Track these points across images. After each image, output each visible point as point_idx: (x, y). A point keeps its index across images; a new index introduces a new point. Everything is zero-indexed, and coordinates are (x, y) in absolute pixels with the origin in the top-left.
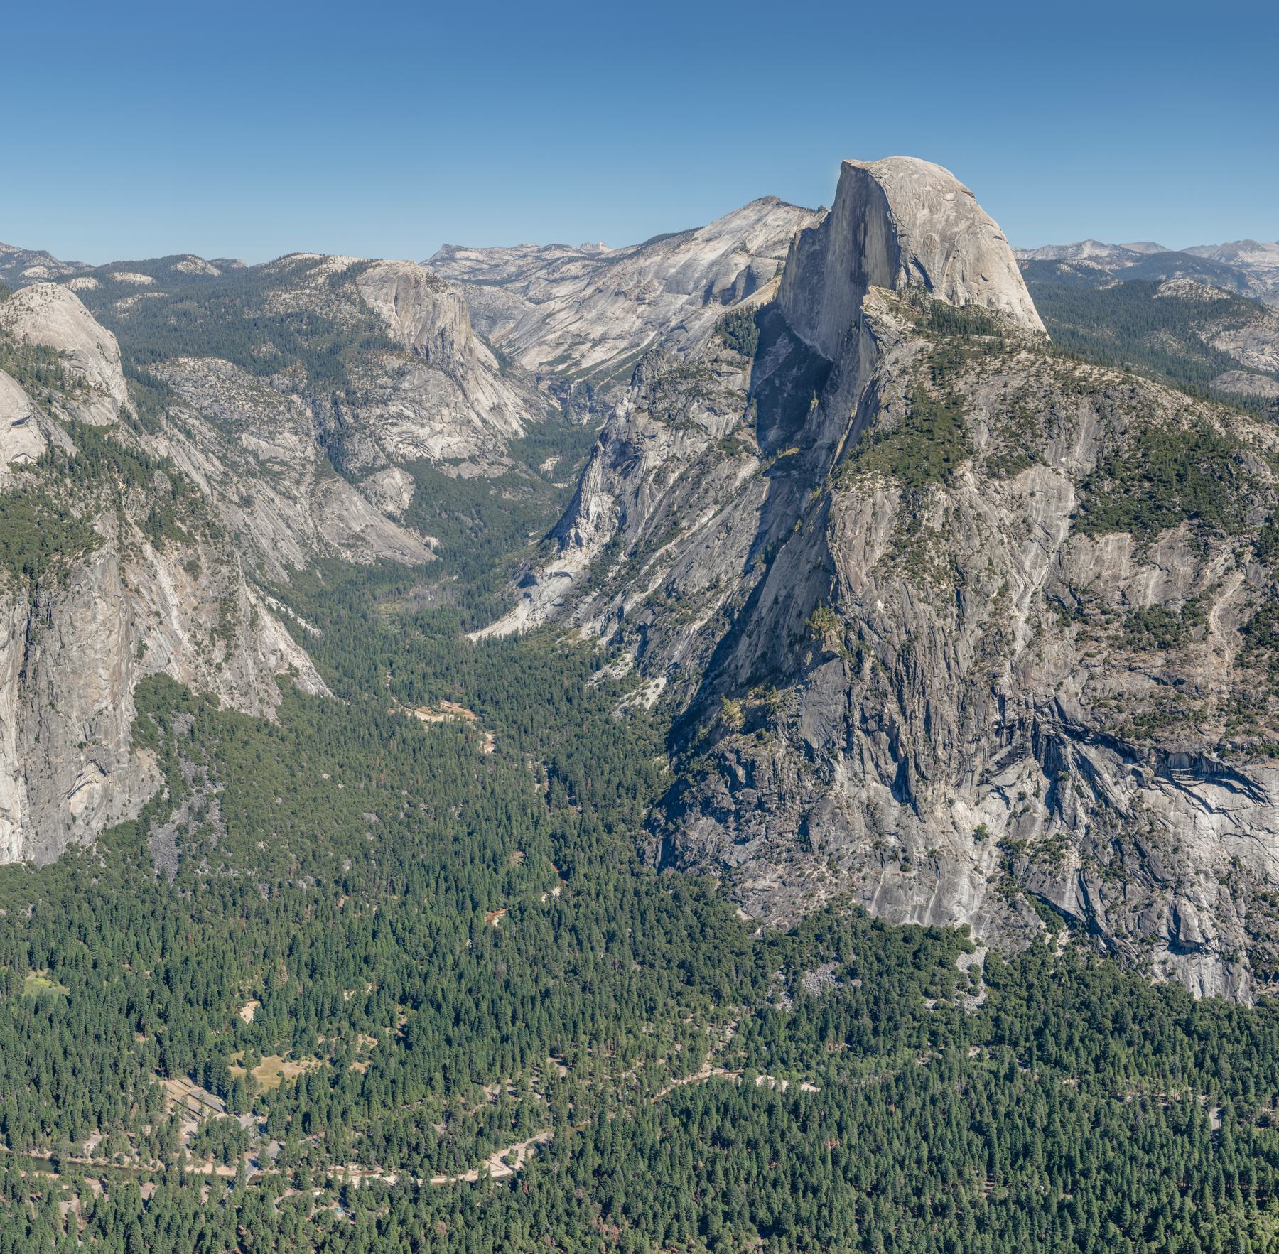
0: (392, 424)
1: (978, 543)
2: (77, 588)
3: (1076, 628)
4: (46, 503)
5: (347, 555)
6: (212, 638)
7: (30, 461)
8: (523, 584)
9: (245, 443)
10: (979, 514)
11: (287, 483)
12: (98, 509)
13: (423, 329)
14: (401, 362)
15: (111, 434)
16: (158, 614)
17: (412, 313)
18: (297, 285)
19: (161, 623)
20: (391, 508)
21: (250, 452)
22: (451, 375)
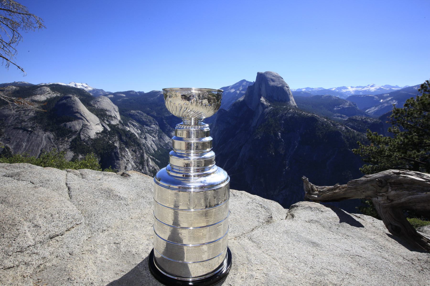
4: (104, 140)
7: (100, 132)
11: (153, 134)
12: (115, 141)
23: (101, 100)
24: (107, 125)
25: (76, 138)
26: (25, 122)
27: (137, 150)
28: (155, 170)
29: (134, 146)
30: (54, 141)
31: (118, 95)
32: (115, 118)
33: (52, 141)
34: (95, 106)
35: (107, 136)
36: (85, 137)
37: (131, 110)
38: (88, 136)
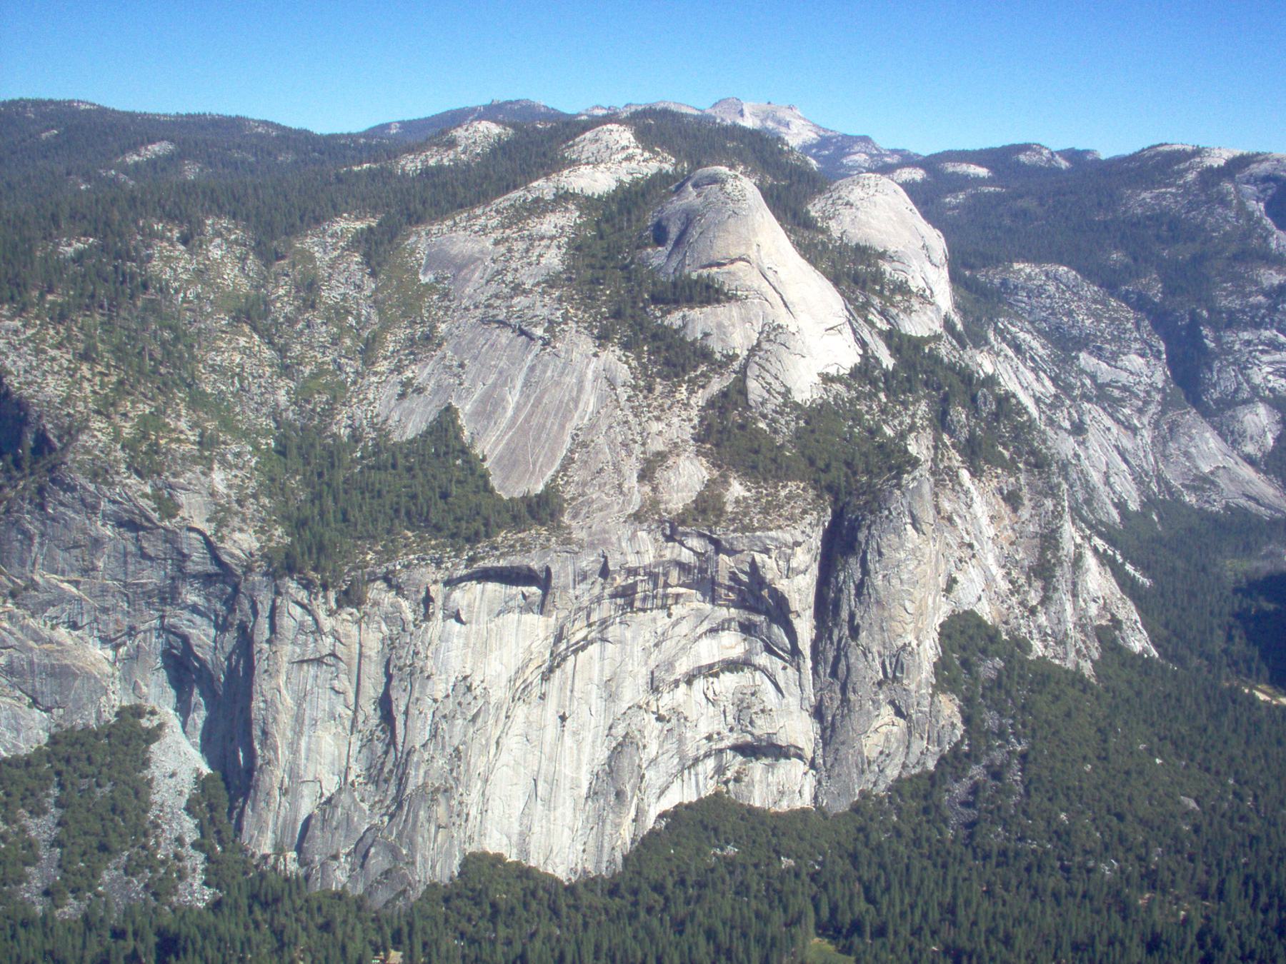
0: (1262, 352)
4: (857, 418)
5: (1190, 499)
6: (1028, 578)
7: (842, 372)
11: (1127, 411)
12: (912, 428)
15: (933, 345)
18: (1159, 182)
19: (974, 556)
20: (1250, 448)
21: (1085, 372)
23: (862, 195)
24: (881, 333)
25: (724, 394)
26: (524, 291)
28: (1116, 623)
29: (1010, 467)
30: (629, 399)
31: (950, 168)
32: (926, 298)
33: (623, 393)
34: (828, 227)
35: (876, 395)
36: (768, 391)
37: (1011, 262)
38: (783, 390)
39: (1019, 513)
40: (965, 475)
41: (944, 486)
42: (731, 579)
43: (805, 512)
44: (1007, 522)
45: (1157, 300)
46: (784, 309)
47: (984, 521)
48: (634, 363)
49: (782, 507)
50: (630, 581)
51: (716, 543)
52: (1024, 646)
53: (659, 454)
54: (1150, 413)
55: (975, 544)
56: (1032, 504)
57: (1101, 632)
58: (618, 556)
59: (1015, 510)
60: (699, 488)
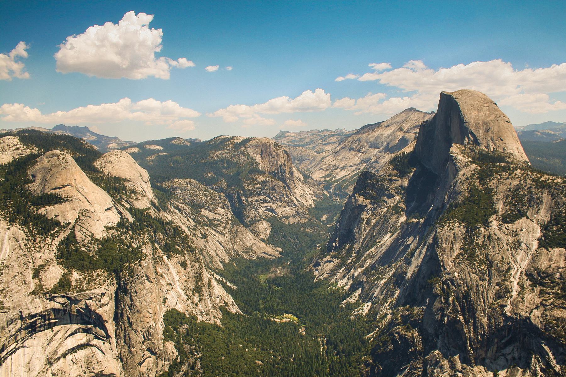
0: (262, 203)
1: (498, 250)
2: (137, 276)
3: (538, 289)
4: (122, 242)
5: (245, 256)
6: (193, 293)
7: (114, 225)
8: (314, 266)
9: (203, 213)
10: (498, 238)
12: (143, 243)
13: (272, 165)
14: (264, 178)
16: (171, 284)
17: (268, 158)
19: (172, 288)
20: (262, 236)
21: (205, 216)
22: (285, 183)
23: (115, 158)
24: (127, 209)
27: (188, 262)
28: (226, 304)
29: (182, 253)
30: (25, 245)
31: (148, 147)
32: (143, 194)
35: (128, 232)
36: (85, 236)
38: (91, 234)
39: (187, 270)
40: (165, 258)
41: (158, 263)
42: (77, 312)
43: (105, 281)
44: (183, 273)
45: (225, 189)
46: (88, 203)
47: (174, 274)
48: (26, 230)
49: (96, 280)
50: (33, 320)
51: (69, 298)
52: (195, 318)
53: (41, 265)
54: (228, 228)
55: (172, 283)
56: (191, 265)
57: (221, 308)
58: (27, 311)
59: (185, 269)
60: (60, 277)
